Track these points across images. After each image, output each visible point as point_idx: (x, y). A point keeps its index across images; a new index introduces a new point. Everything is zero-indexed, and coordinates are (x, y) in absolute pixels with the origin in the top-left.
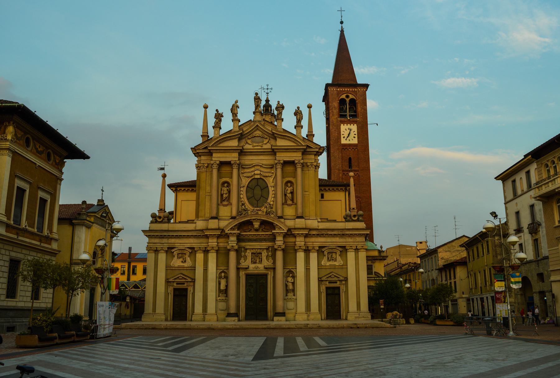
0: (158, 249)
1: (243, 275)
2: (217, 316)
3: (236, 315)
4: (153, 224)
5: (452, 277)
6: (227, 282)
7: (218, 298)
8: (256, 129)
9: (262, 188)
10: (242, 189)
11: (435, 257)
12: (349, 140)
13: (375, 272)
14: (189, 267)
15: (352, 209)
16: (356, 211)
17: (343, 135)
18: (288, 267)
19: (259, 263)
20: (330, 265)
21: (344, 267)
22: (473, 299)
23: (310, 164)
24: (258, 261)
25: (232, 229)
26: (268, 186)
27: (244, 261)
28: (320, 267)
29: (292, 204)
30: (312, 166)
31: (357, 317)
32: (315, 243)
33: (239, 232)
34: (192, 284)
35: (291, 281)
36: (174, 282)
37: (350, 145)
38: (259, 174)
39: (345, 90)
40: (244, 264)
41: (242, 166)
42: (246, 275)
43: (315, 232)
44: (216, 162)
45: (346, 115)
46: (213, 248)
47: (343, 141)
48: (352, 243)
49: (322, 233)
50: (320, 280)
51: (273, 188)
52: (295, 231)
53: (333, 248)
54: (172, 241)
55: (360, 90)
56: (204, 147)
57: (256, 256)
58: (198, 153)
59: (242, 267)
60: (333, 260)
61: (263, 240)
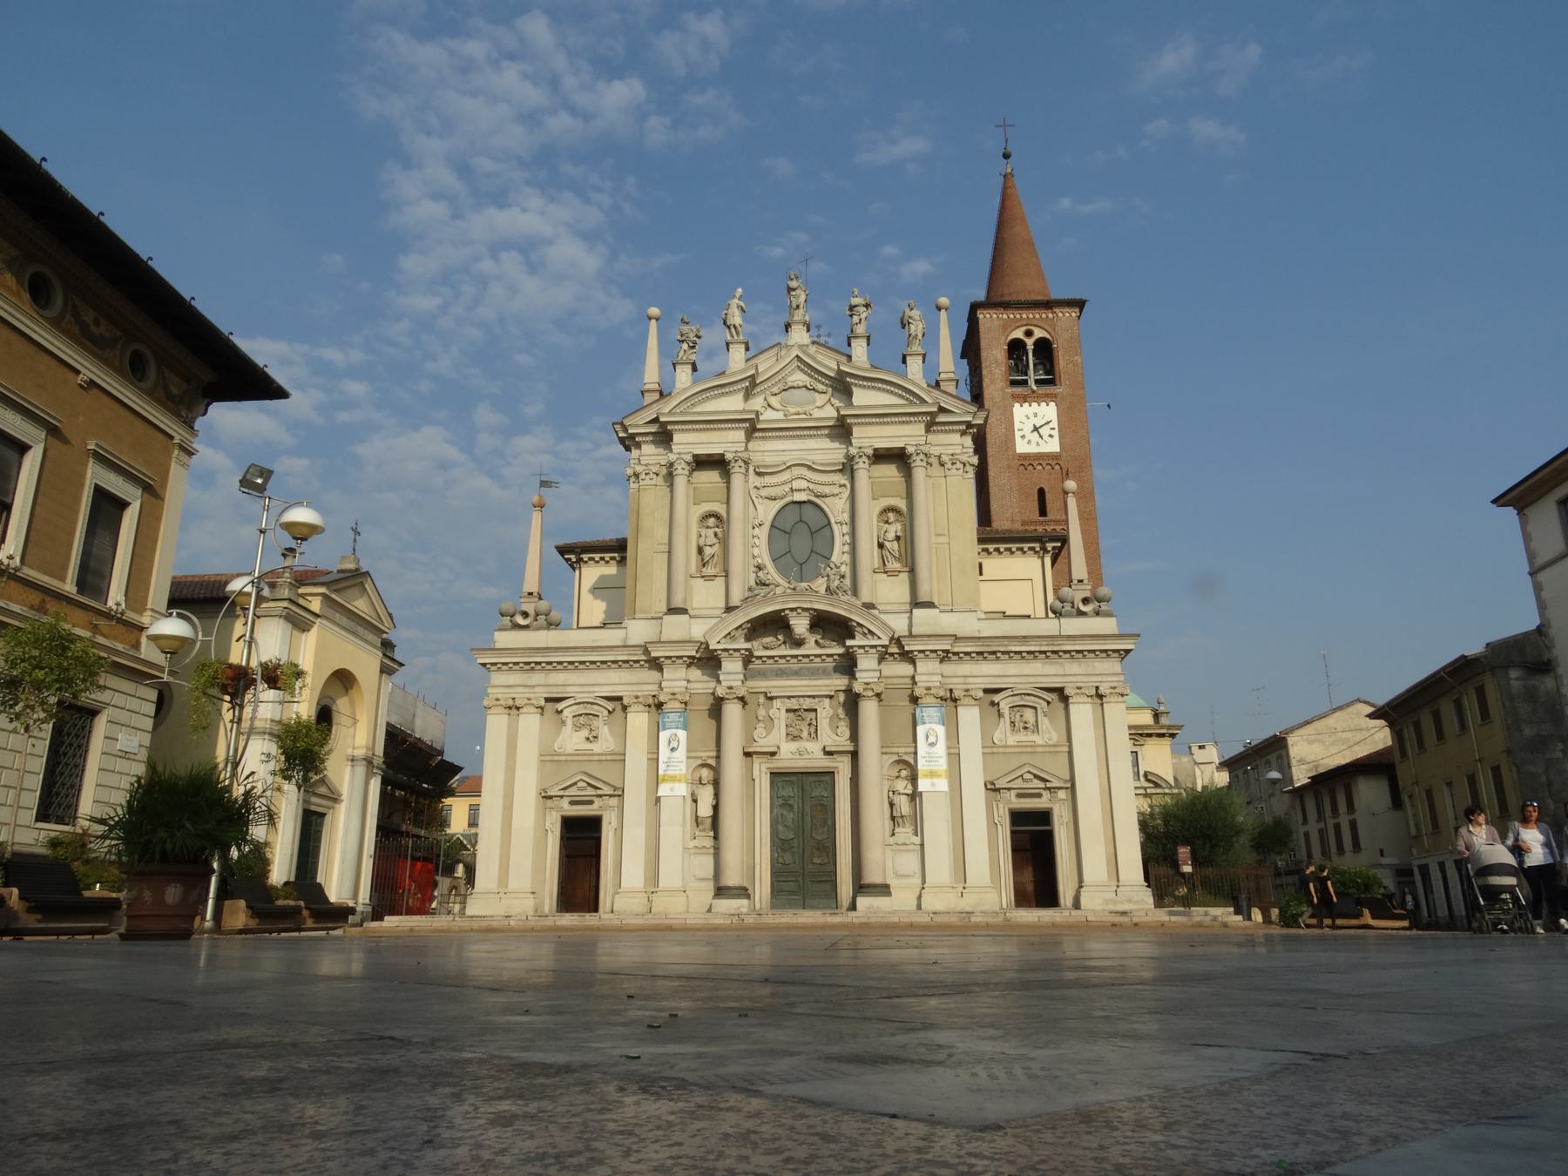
0: (518, 703)
1: (763, 775)
2: (687, 896)
3: (743, 892)
4: (504, 633)
5: (1342, 807)
6: (717, 795)
7: (692, 844)
8: (793, 367)
9: (813, 530)
10: (756, 532)
11: (1280, 757)
13: (1146, 774)
14: (606, 755)
15: (1075, 582)
16: (1089, 587)
17: (1019, 430)
18: (895, 750)
19: (807, 740)
20: (1020, 745)
21: (1060, 749)
22: (1424, 870)
23: (950, 460)
24: (805, 734)
26: (829, 524)
27: (764, 735)
28: (990, 749)
29: (900, 572)
30: (953, 464)
31: (1110, 900)
32: (971, 680)
33: (748, 646)
34: (614, 801)
35: (906, 791)
36: (562, 797)
37: (1040, 457)
38: (804, 490)
40: (764, 742)
41: (755, 470)
42: (771, 773)
44: (682, 456)
45: (1025, 383)
46: (676, 696)
47: (1022, 447)
48: (1084, 679)
49: (988, 651)
50: (992, 789)
51: (844, 526)
52: (911, 643)
53: (1025, 694)
54: (559, 677)
55: (1060, 315)
56: (648, 420)
57: (802, 715)
58: (632, 437)
59: (758, 750)
60: (1026, 728)
61: (820, 671)
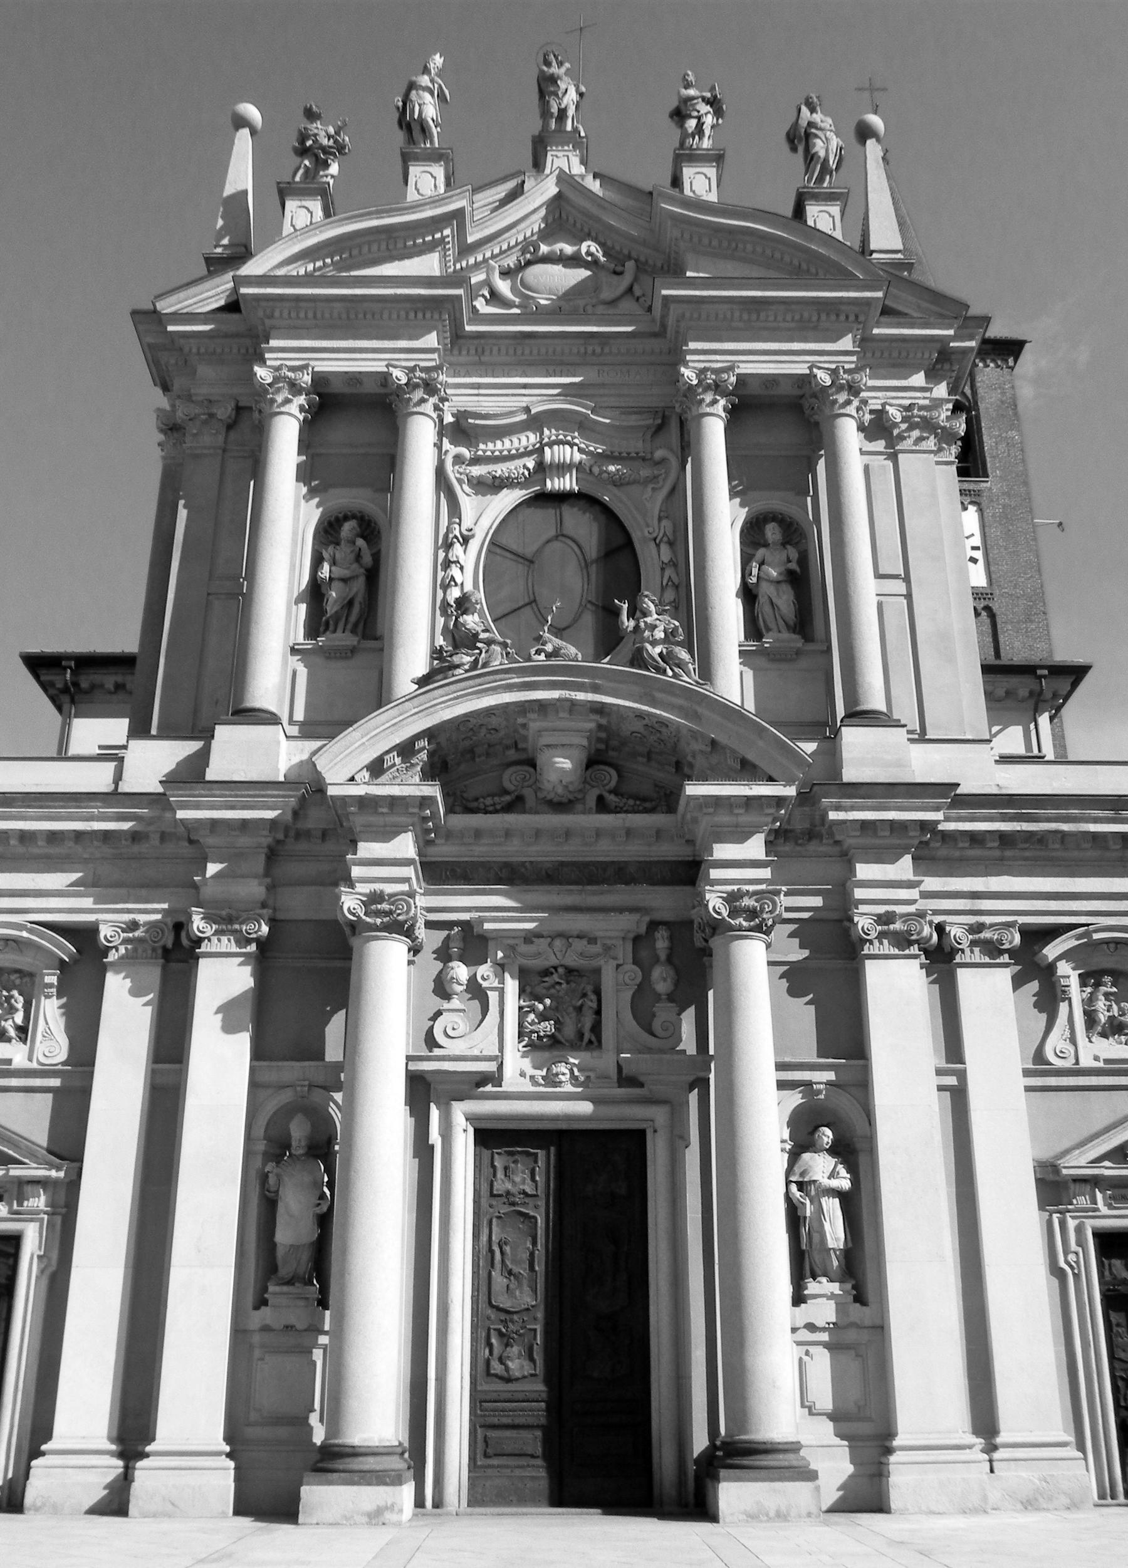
25: (377, 768)
26: (629, 544)
35: (835, 1183)
51: (665, 549)
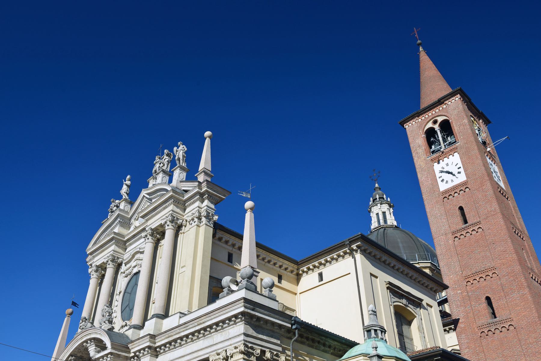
12: (452, 181)
17: (439, 178)
39: (428, 116)
43: (164, 339)
47: (443, 187)
55: (450, 103)
